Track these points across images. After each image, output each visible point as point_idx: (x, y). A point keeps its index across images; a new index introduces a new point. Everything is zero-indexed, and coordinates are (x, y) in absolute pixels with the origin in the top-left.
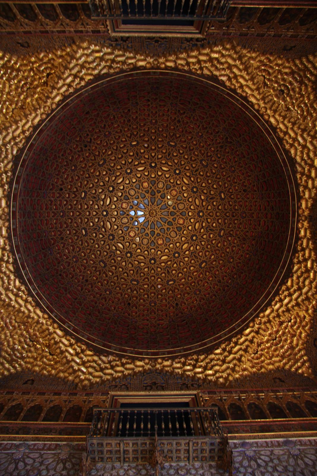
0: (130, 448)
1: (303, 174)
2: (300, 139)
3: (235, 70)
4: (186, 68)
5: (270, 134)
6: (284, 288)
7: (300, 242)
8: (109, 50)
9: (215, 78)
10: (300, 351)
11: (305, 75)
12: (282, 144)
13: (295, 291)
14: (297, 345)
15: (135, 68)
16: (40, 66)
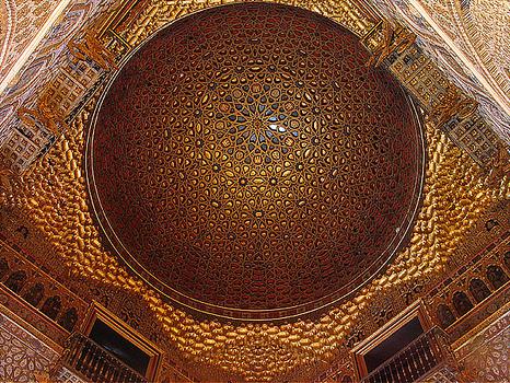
0: (72, 91)
1: (182, 319)
2: (211, 341)
3: (307, 340)
4: (344, 306)
5: (236, 314)
6: (96, 233)
7: (126, 274)
8: (415, 275)
9: (316, 318)
10: (23, 202)
11: (256, 376)
12: (220, 320)
13: (86, 244)
14: (29, 202)
15: (383, 273)
16: (467, 210)
